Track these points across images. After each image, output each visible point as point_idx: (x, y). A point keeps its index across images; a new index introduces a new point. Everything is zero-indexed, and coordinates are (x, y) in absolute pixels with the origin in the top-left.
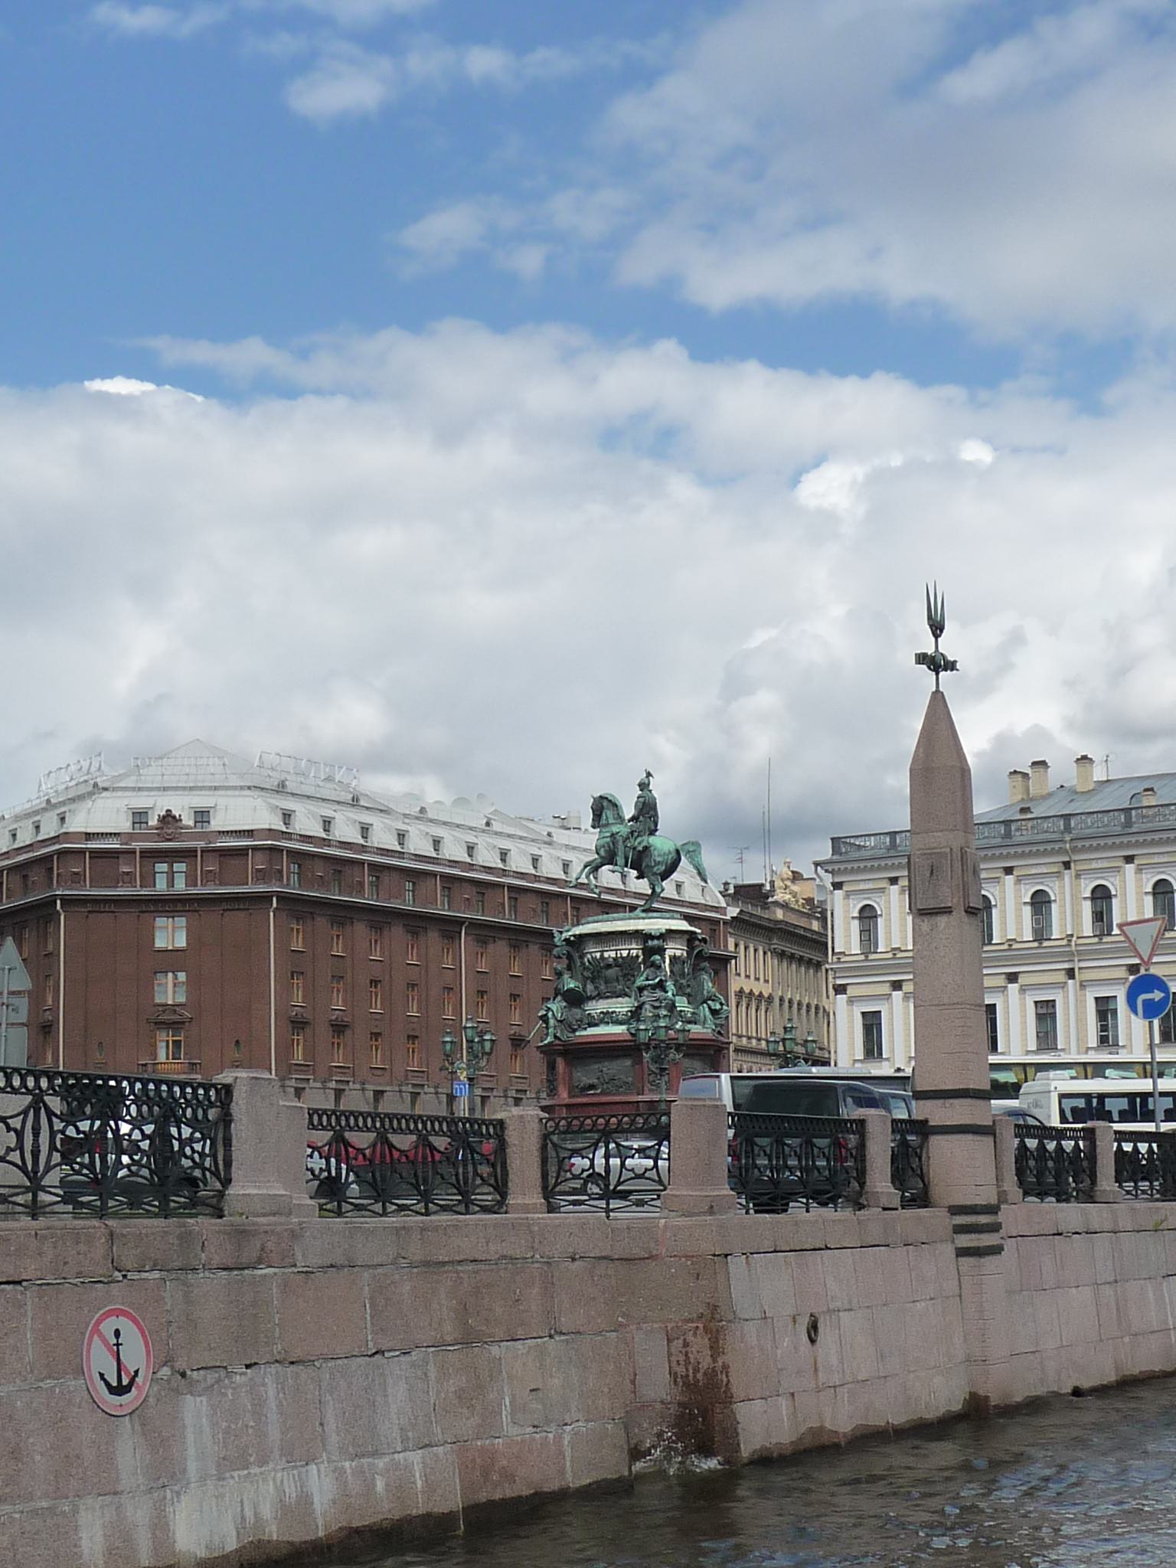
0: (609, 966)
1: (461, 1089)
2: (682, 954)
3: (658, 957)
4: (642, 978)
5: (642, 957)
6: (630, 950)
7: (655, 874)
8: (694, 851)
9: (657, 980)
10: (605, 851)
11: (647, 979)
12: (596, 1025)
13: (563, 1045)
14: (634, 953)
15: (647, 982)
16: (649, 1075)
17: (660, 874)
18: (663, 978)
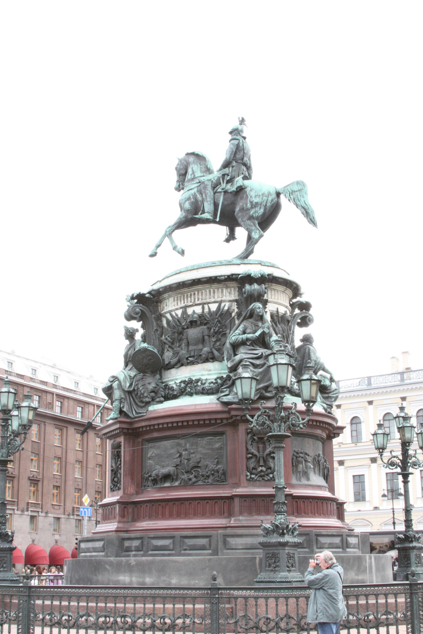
0: (193, 323)
1: (85, 512)
2: (286, 312)
3: (258, 305)
4: (237, 332)
5: (236, 310)
6: (220, 302)
7: (251, 218)
8: (300, 190)
9: (258, 334)
10: (192, 204)
11: (244, 333)
12: (175, 397)
13: (131, 423)
14: (226, 306)
15: (244, 336)
16: (248, 459)
17: (257, 218)
18: (266, 331)
